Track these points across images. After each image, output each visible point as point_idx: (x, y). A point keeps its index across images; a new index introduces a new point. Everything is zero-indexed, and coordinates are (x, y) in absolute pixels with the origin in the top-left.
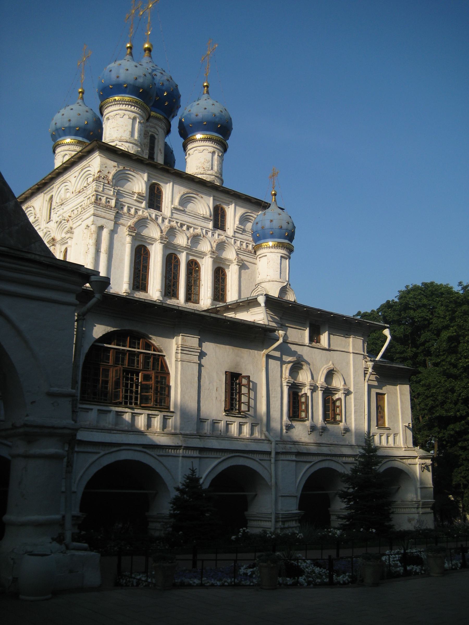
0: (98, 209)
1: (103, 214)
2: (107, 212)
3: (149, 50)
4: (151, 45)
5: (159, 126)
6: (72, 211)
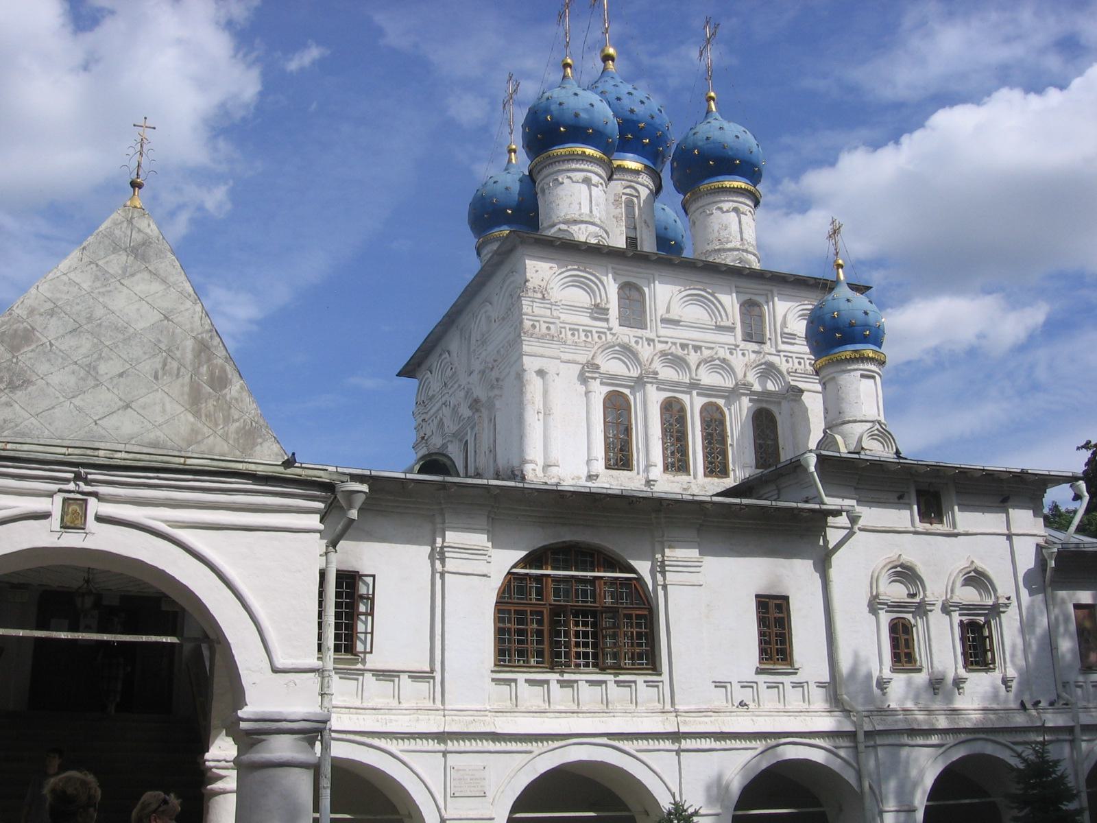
1: (540, 351)
2: (547, 345)
5: (638, 183)
6: (498, 352)
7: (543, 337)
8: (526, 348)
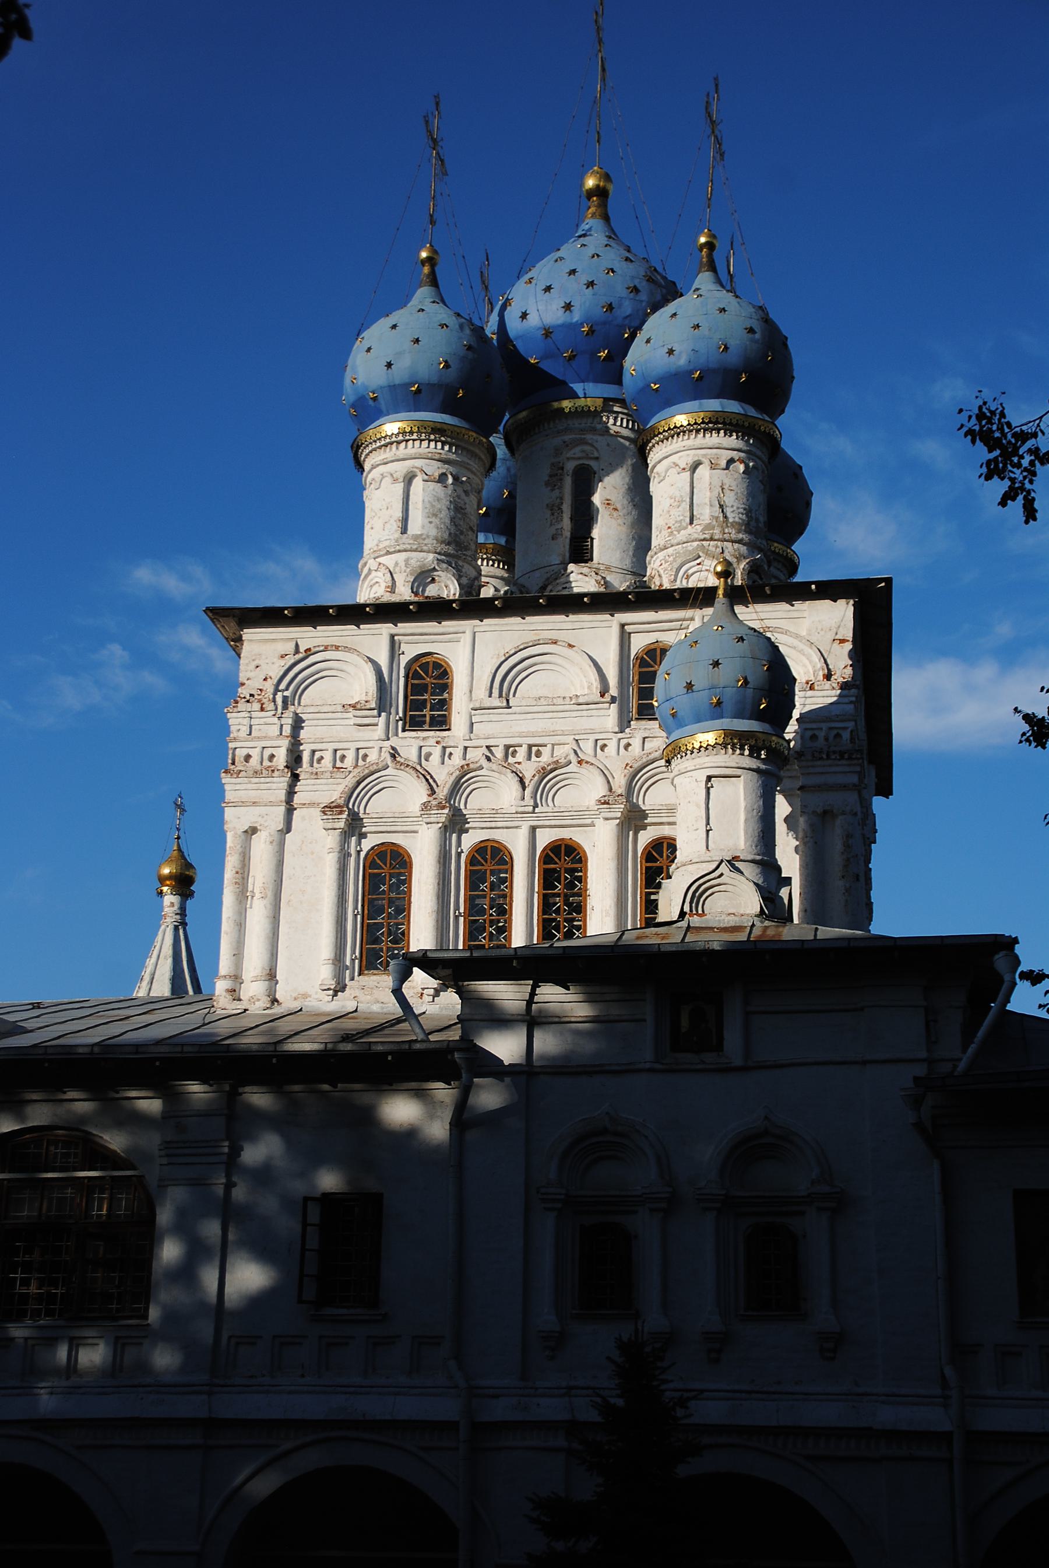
0: (238, 787)
2: (263, 786)
3: (600, 192)
4: (607, 177)
7: (256, 773)
8: (229, 796)
